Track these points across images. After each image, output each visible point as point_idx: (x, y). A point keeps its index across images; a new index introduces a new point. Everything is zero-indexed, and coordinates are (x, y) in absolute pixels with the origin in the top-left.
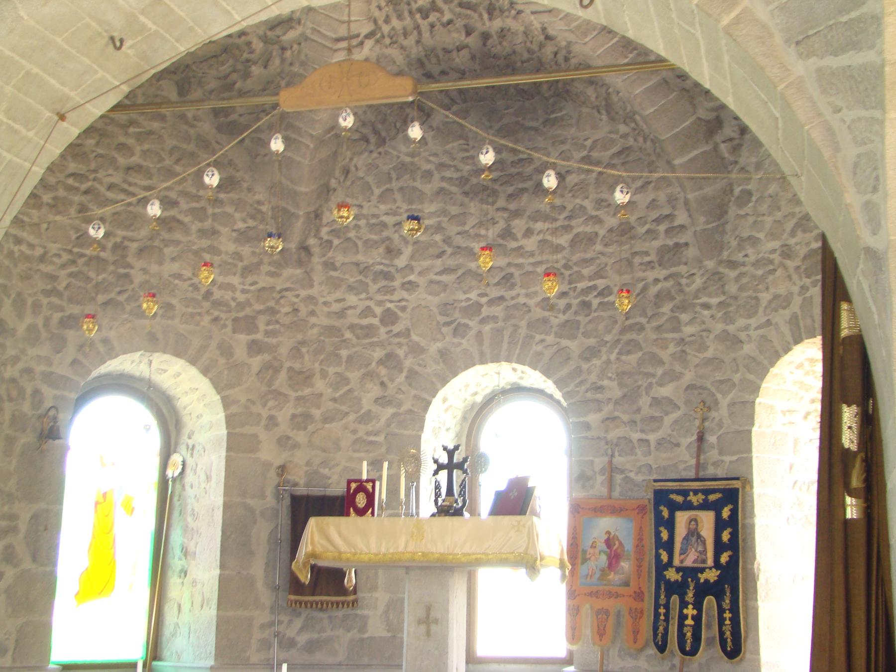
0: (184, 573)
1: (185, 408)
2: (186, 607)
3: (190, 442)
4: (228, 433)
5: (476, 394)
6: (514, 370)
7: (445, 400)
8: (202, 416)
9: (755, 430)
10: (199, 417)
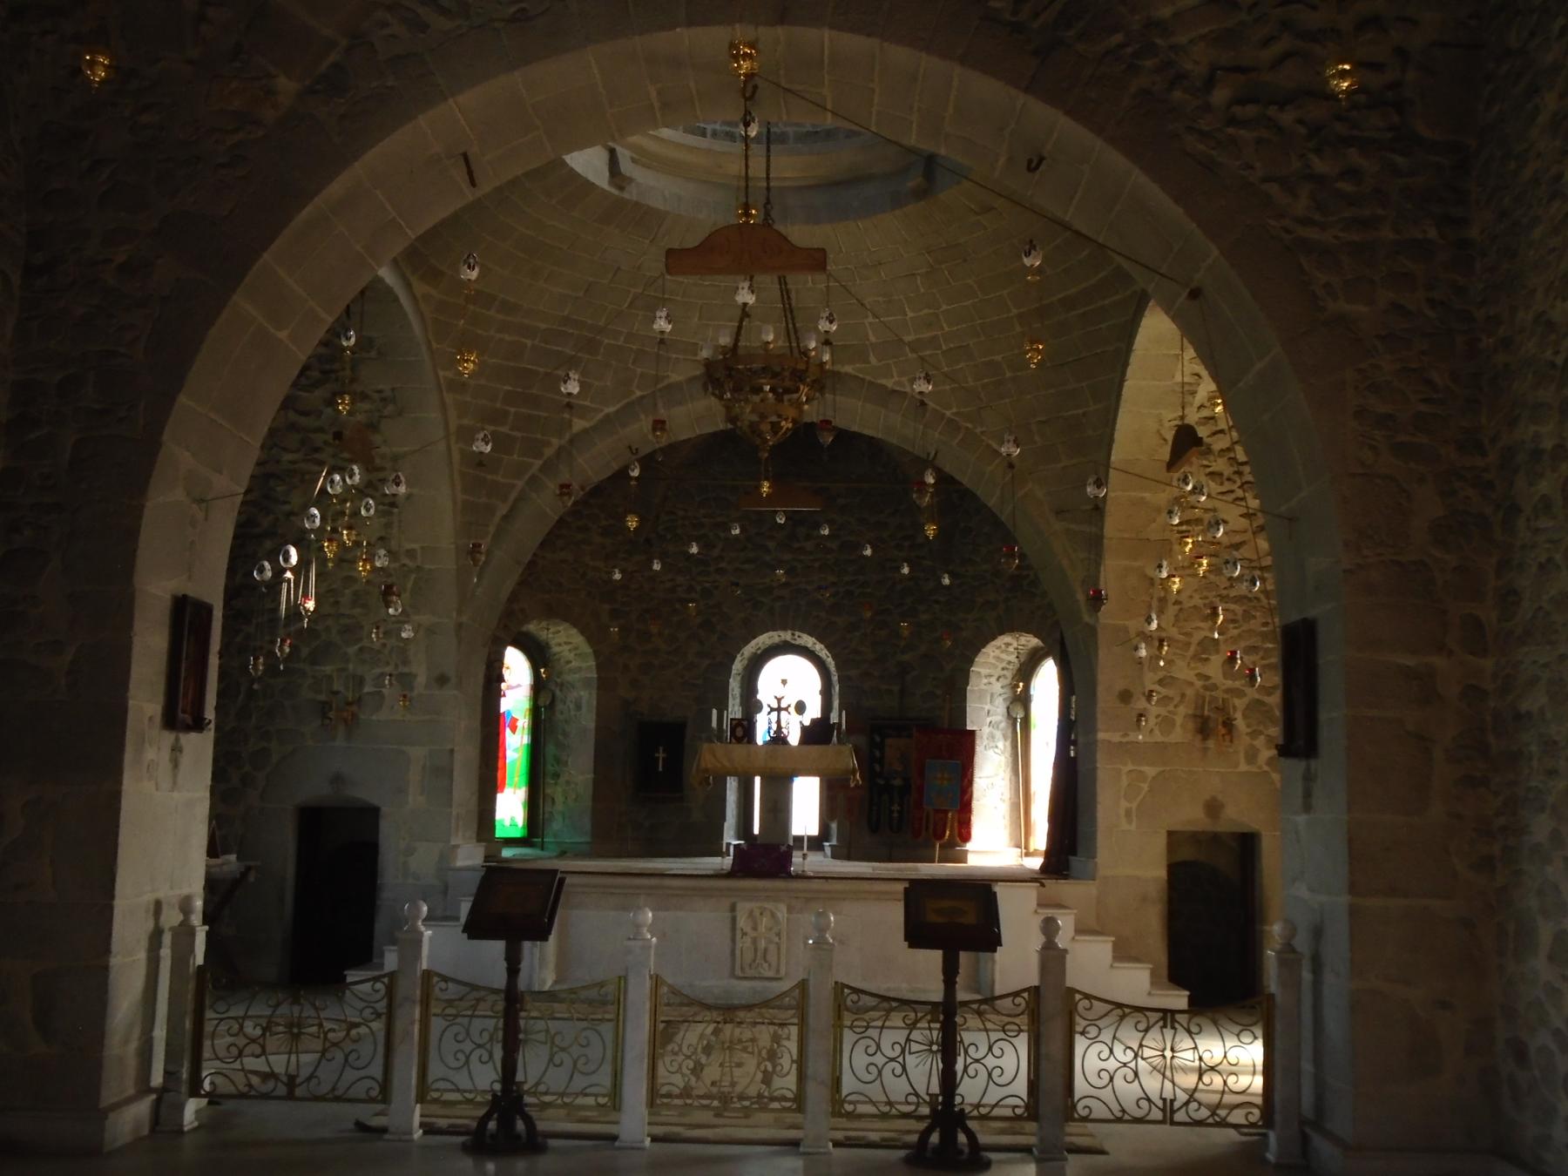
0: (556, 776)
1: (555, 655)
2: (559, 799)
3: (559, 680)
4: (599, 678)
5: (759, 648)
6: (793, 635)
7: (742, 655)
8: (571, 662)
9: (969, 688)
10: (569, 662)
